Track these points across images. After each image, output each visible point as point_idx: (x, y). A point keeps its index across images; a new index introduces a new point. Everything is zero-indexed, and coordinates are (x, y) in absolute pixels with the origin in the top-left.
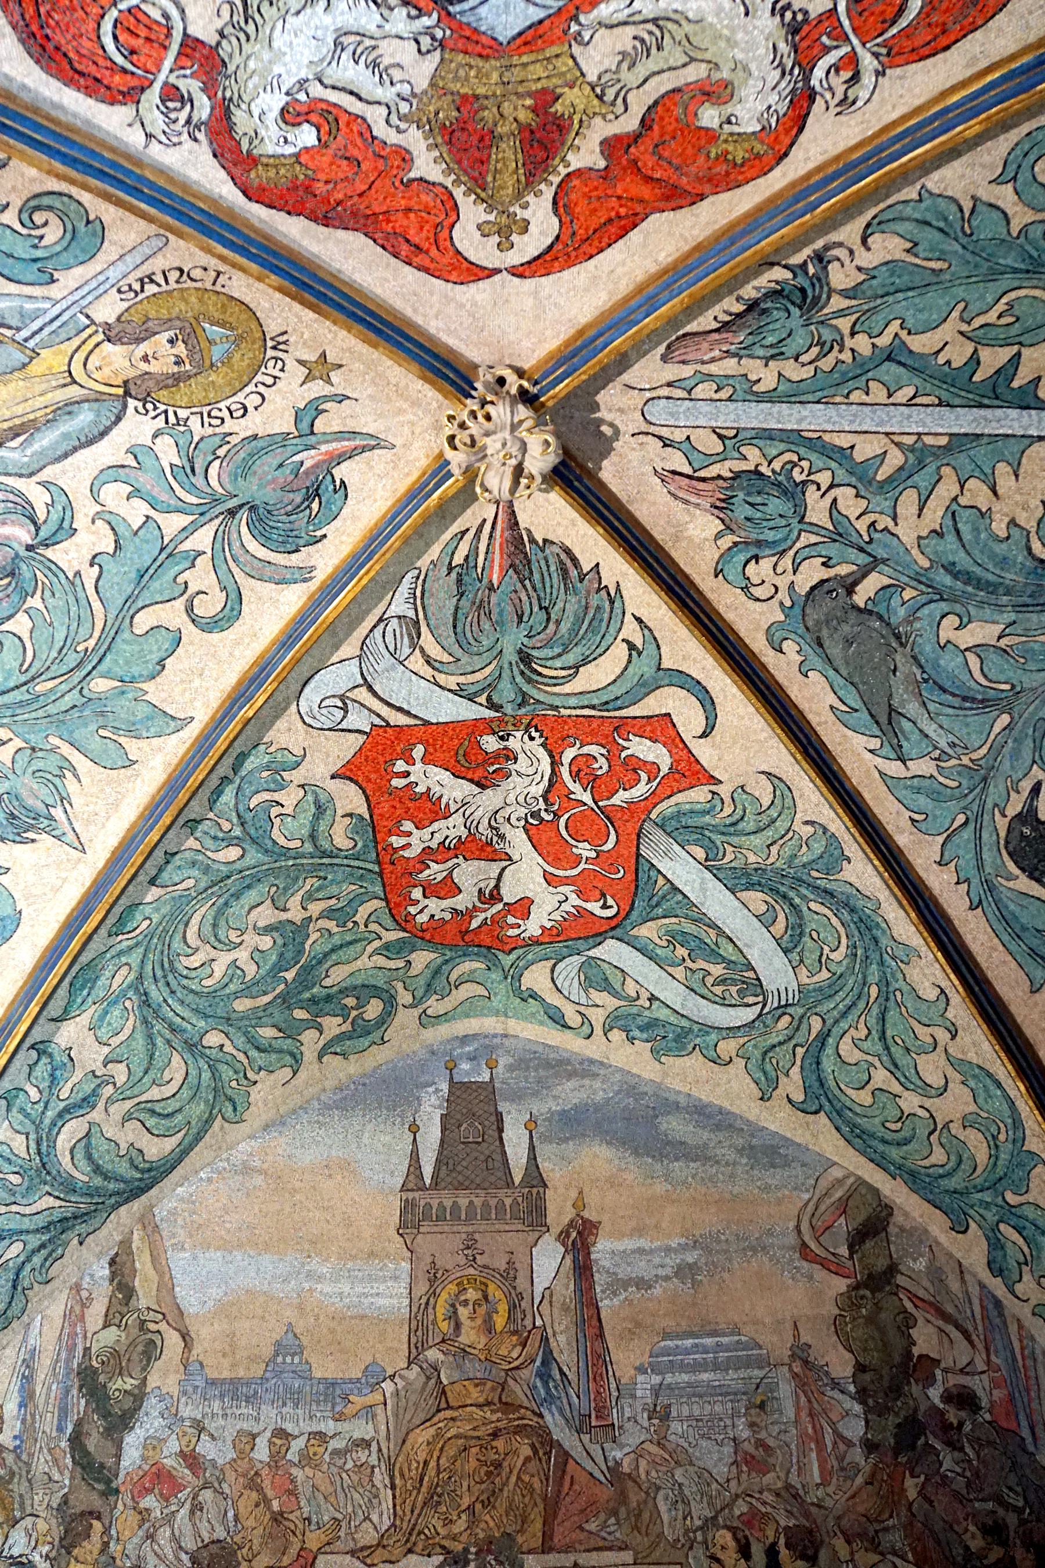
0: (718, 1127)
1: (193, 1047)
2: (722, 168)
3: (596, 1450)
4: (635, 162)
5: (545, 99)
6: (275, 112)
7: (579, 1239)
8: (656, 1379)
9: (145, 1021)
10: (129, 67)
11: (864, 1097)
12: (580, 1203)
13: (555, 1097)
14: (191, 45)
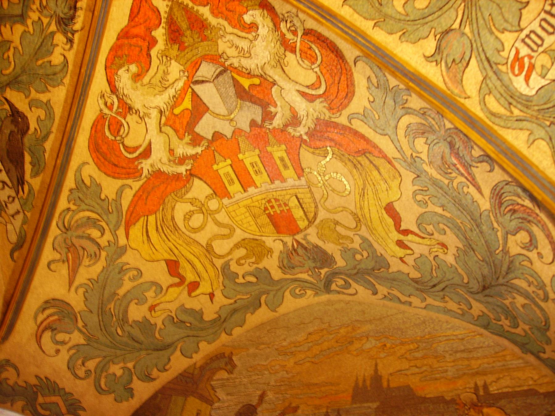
2: (119, 53)
4: (144, 40)
5: (182, 48)
6: (260, 27)
10: (310, 44)
14: (293, 51)
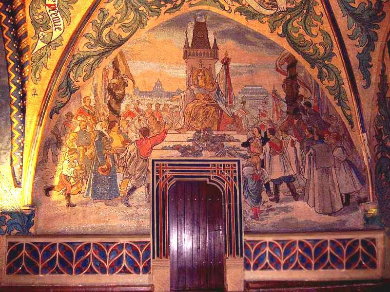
0: (259, 38)
1: (136, 10)
3: (229, 110)
7: (226, 62)
8: (243, 95)
9: (127, 4)
11: (296, 35)
12: (226, 54)
13: (221, 27)
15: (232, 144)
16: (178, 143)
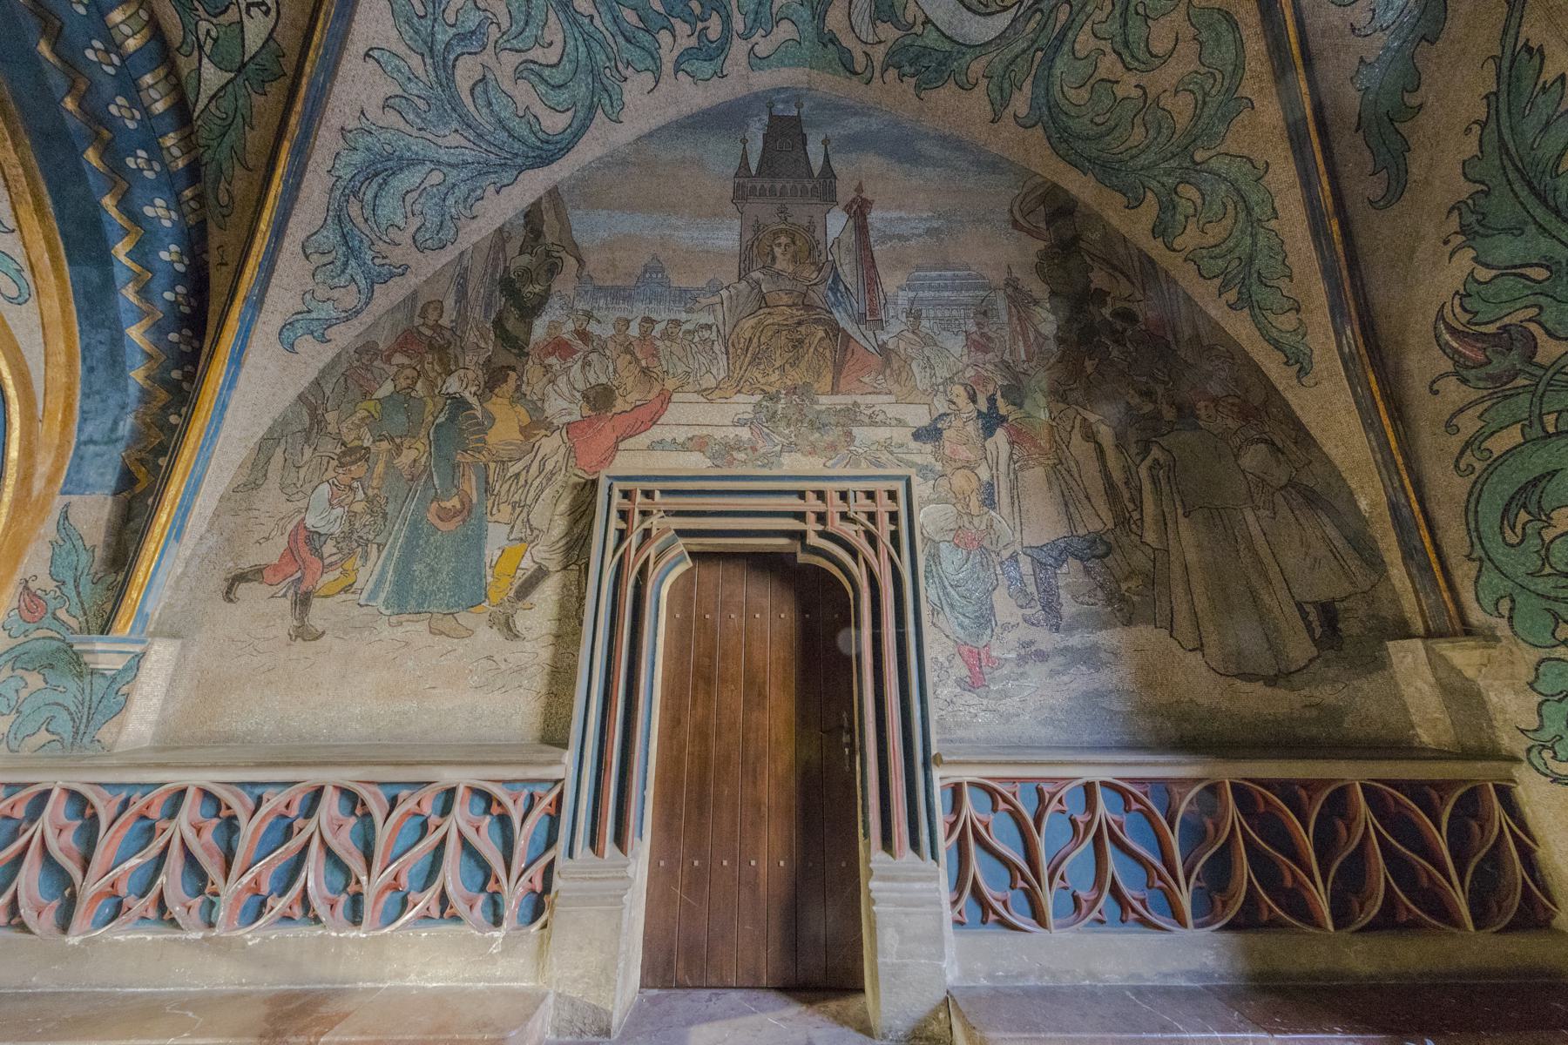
8: (912, 294)
12: (859, 189)
15: (882, 433)
16: (704, 431)
